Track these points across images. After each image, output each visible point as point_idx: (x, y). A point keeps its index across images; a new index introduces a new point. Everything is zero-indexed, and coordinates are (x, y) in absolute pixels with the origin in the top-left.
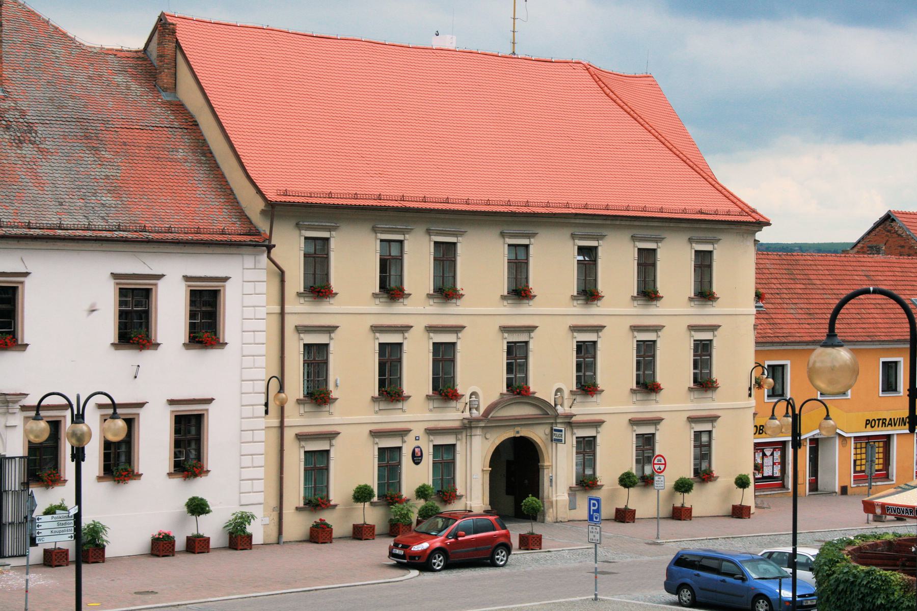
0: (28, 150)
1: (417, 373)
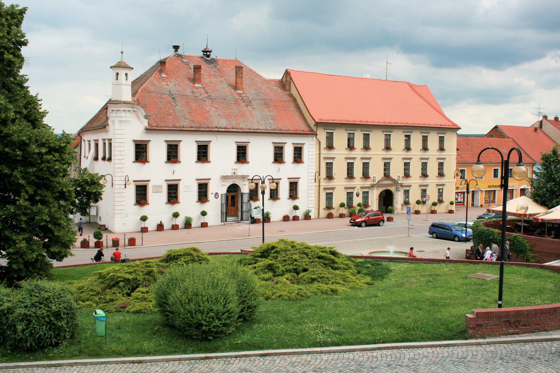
0: (250, 108)
1: (358, 171)
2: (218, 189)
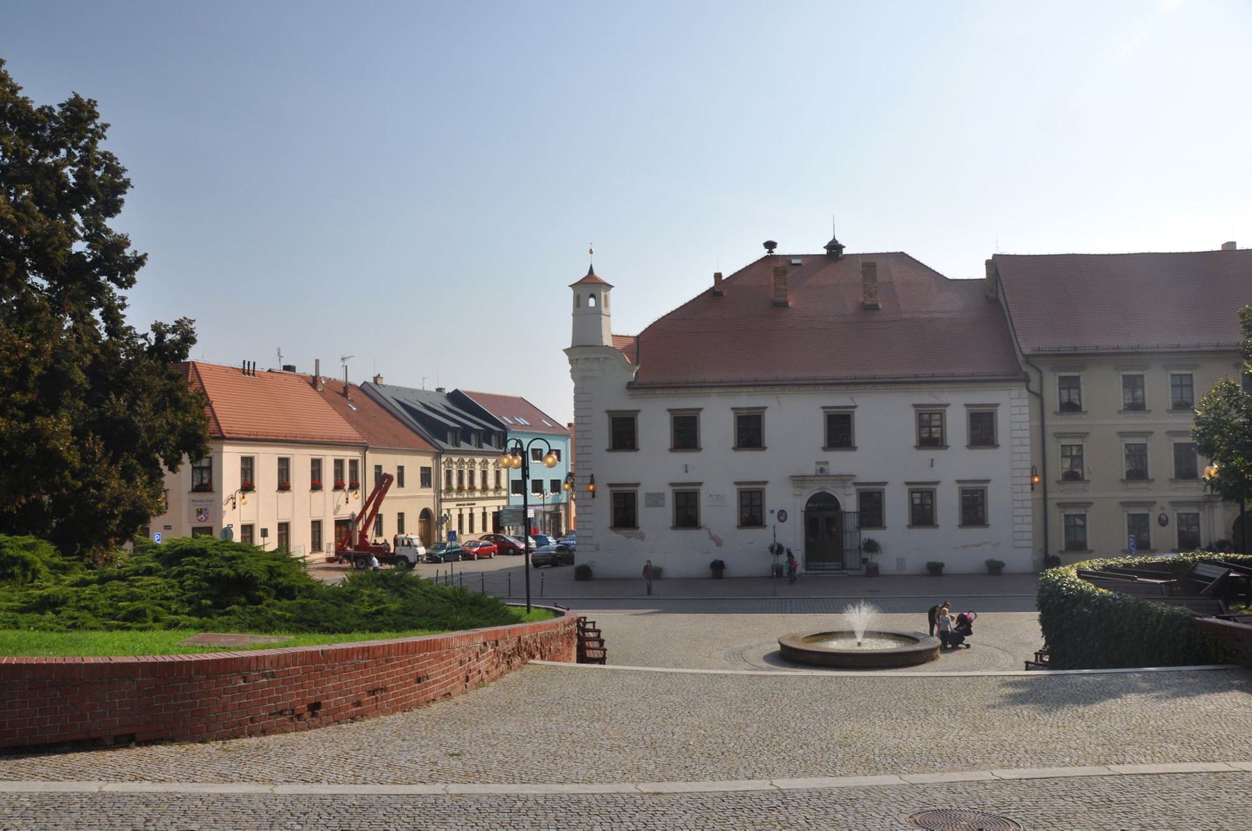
2: (788, 504)
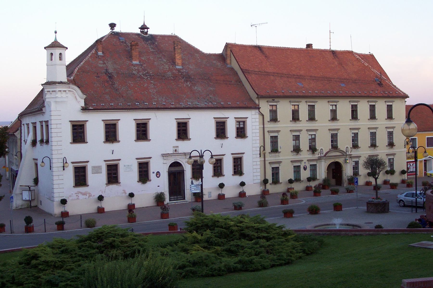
2: (160, 167)
